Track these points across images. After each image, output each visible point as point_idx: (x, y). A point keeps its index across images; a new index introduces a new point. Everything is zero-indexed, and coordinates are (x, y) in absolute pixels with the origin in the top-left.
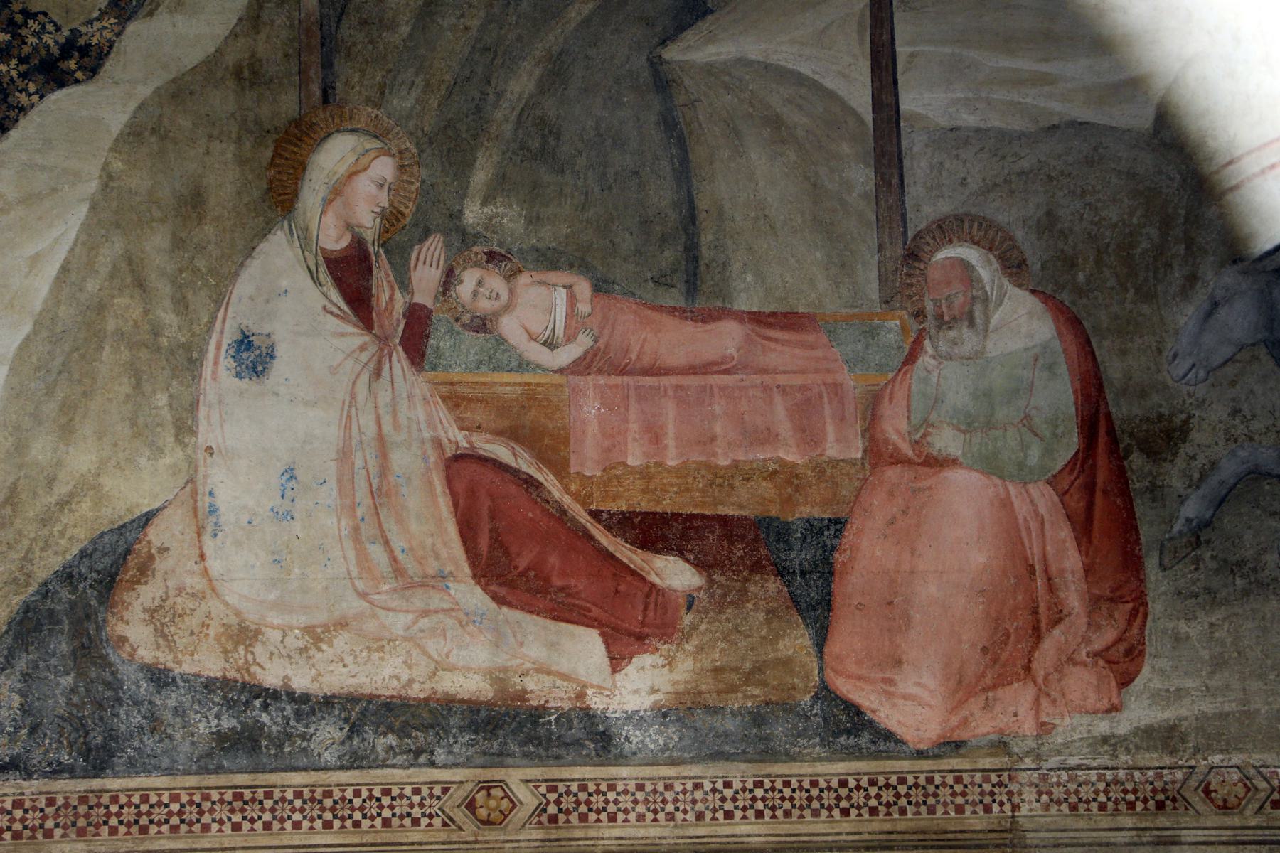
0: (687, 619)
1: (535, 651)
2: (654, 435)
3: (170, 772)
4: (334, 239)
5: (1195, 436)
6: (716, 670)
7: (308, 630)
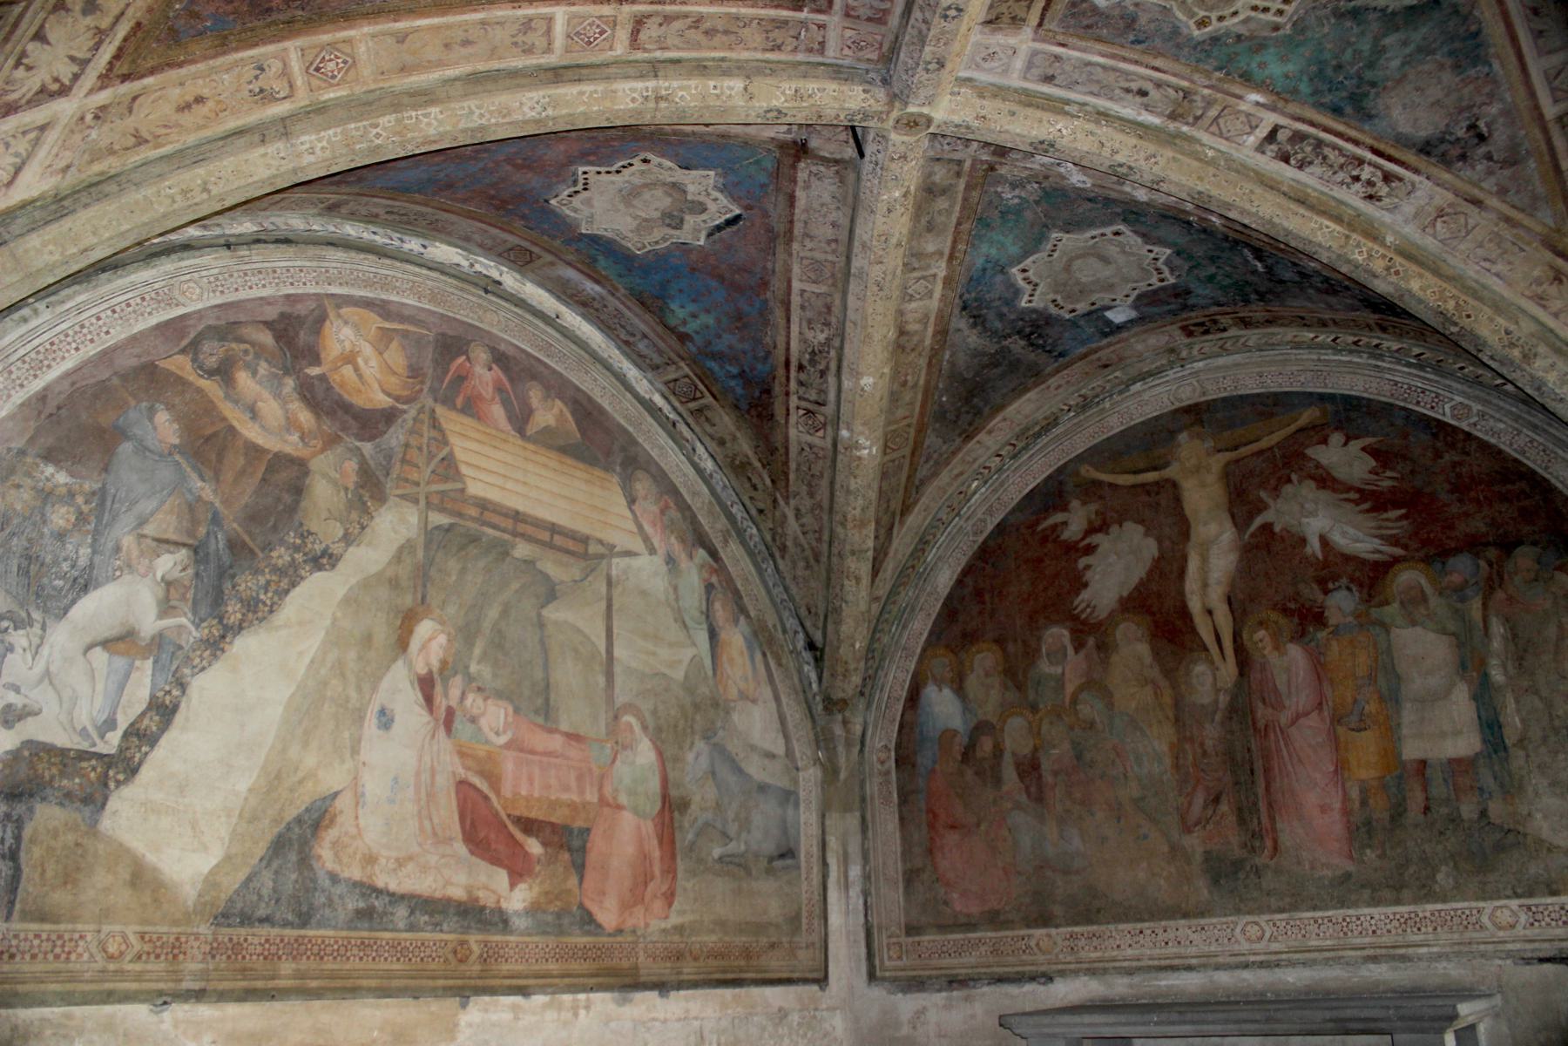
0: (538, 868)
1: (483, 879)
2: (531, 781)
3: (335, 928)
4: (422, 670)
5: (693, 807)
6: (547, 893)
7: (397, 860)
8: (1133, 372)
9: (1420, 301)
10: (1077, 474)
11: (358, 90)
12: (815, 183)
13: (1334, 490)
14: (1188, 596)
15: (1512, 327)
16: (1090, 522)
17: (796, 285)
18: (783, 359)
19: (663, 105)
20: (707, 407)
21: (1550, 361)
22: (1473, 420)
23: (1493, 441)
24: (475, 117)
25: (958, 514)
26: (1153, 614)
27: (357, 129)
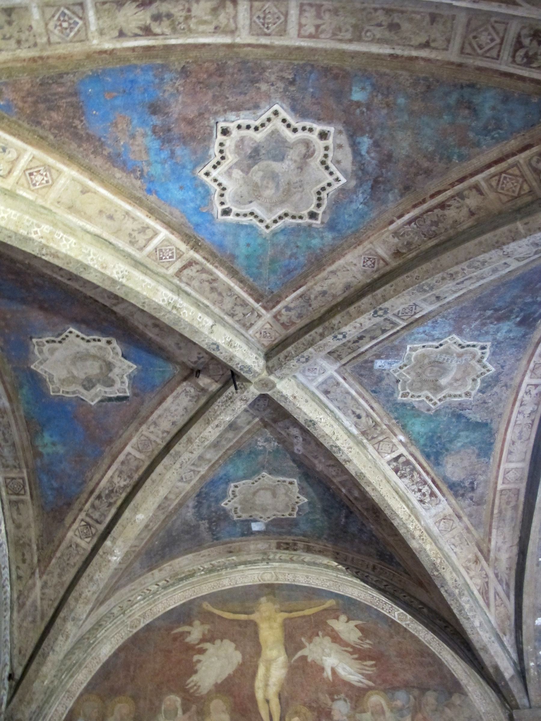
8: (243, 558)
9: (428, 556)
10: (200, 606)
11: (40, 202)
12: (183, 395)
13: (340, 645)
14: (256, 689)
15: (457, 579)
16: (204, 635)
17: (128, 449)
18: (91, 488)
19: (174, 311)
20: (23, 502)
21: (468, 599)
22: (408, 622)
23: (416, 634)
24: (89, 258)
25: (124, 613)
26: (235, 697)
27: (28, 221)
